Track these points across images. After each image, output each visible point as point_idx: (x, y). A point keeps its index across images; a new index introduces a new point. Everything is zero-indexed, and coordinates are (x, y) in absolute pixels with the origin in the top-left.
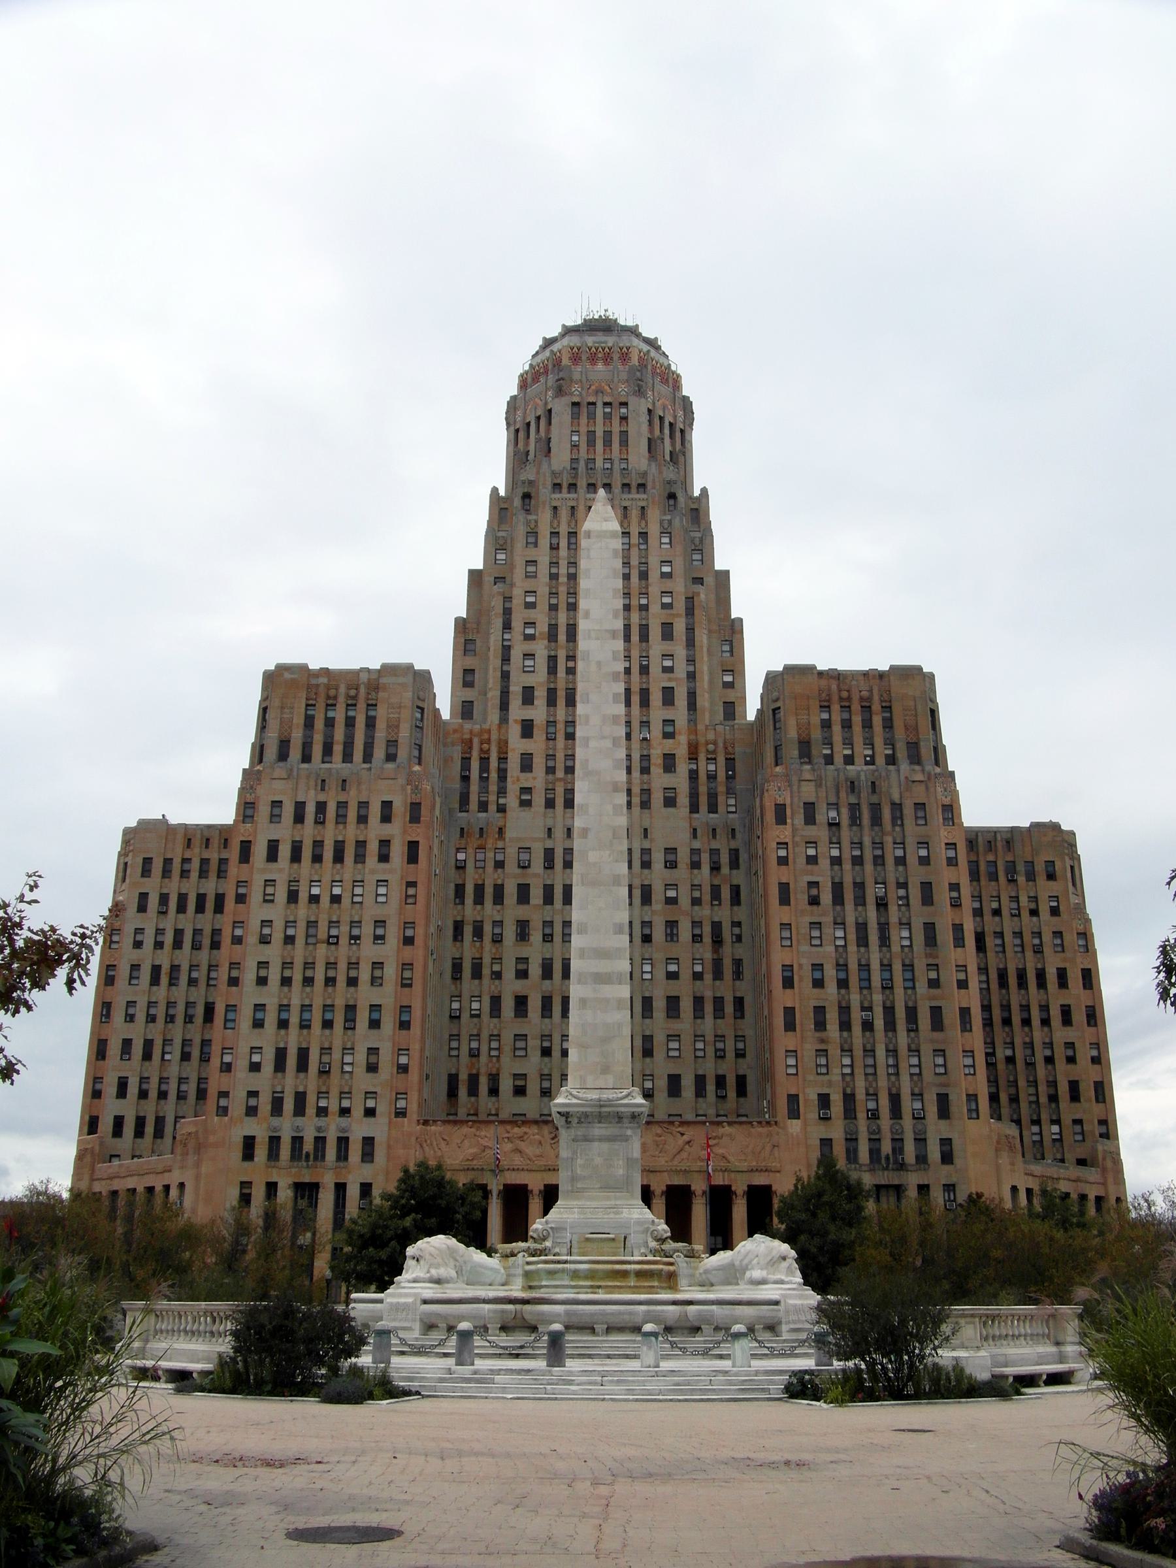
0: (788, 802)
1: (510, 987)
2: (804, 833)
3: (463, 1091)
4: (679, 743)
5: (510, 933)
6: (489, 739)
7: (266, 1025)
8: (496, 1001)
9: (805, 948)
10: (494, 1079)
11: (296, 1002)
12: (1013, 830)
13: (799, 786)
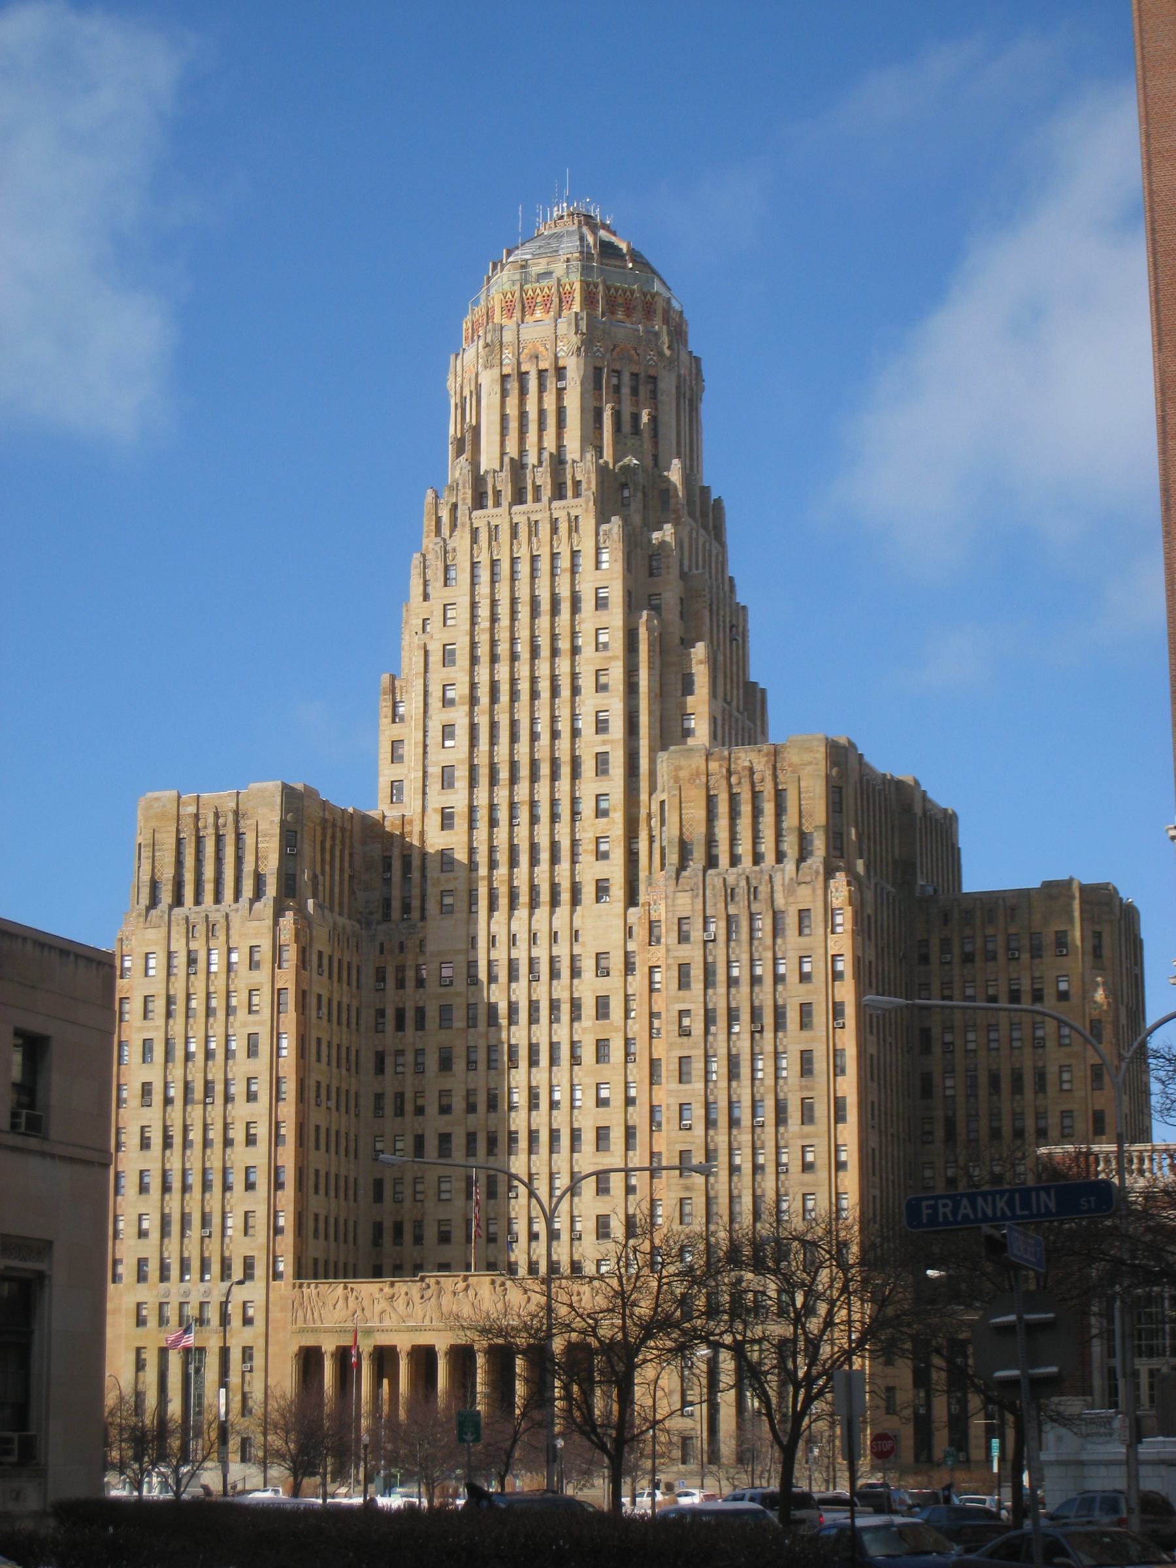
0: (663, 918)
1: (433, 1124)
2: (676, 954)
3: (387, 1238)
4: (614, 823)
5: (432, 1062)
6: (411, 833)
7: (151, 1191)
8: (419, 1142)
9: (674, 1085)
10: (418, 1224)
11: (175, 1164)
12: (1024, 894)
13: (674, 899)
